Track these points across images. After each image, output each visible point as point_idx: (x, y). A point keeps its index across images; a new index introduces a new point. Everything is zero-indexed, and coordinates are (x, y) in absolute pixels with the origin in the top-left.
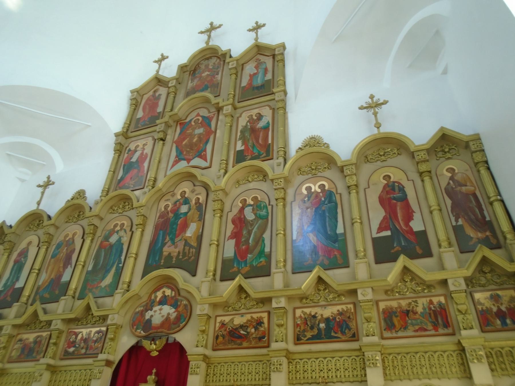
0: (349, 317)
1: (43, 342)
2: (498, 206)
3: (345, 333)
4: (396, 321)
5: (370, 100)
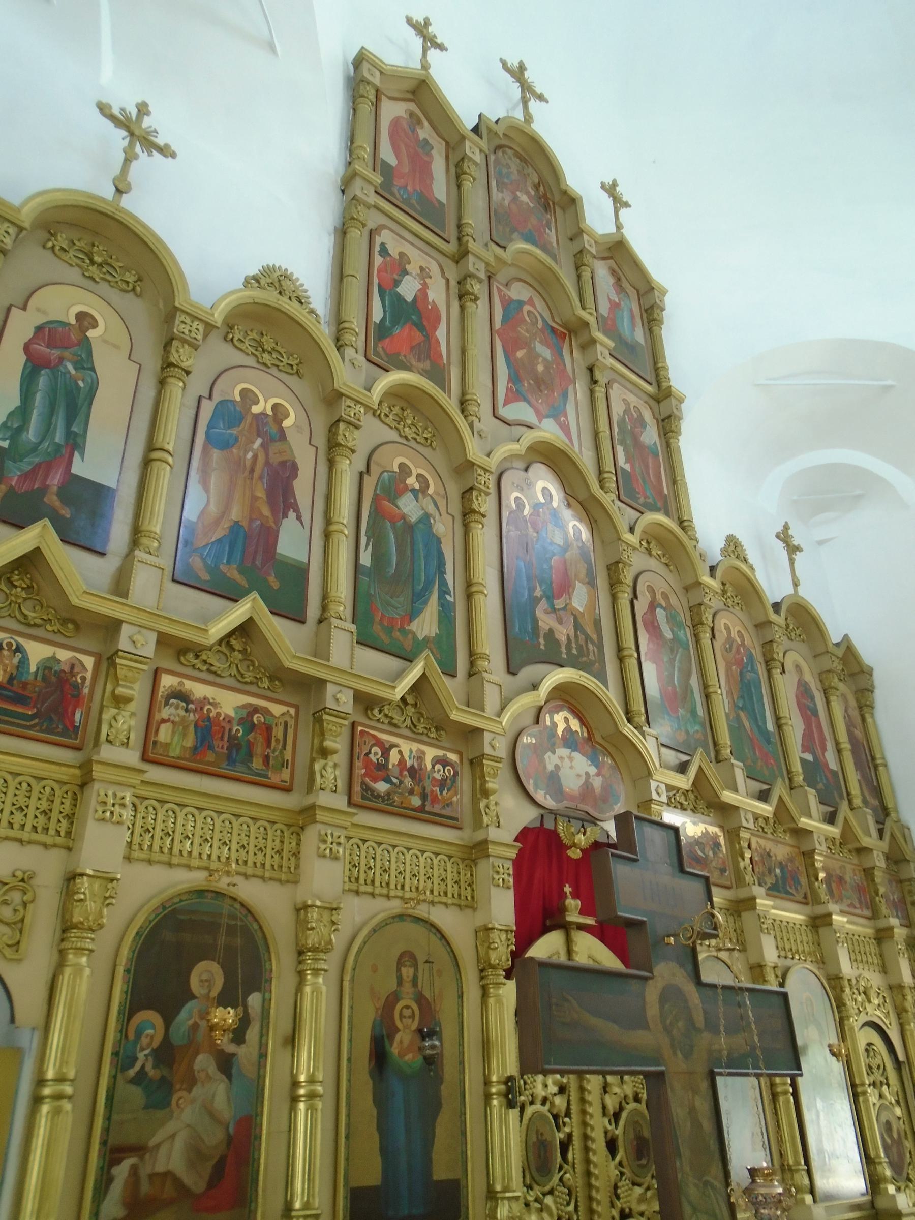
1: (278, 732)
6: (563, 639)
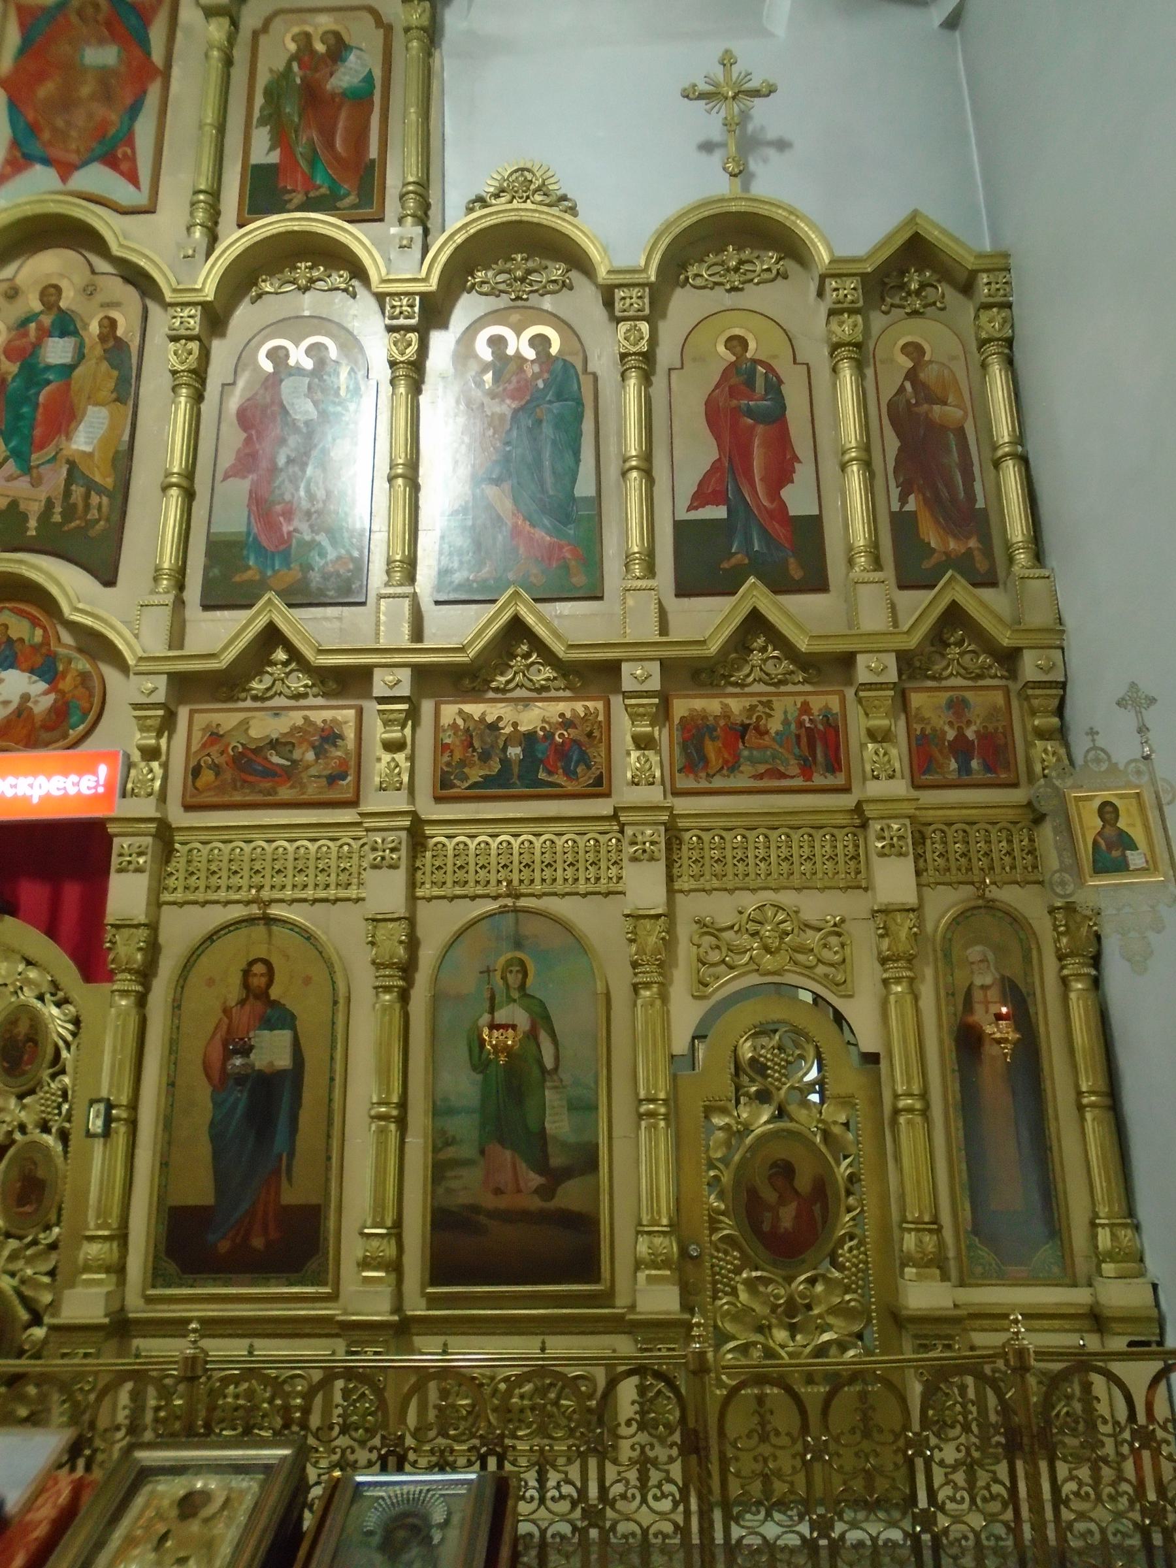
0: (590, 735)
2: (1011, 474)
3: (575, 773)
4: (710, 748)
5: (718, 73)
6: (34, 510)
